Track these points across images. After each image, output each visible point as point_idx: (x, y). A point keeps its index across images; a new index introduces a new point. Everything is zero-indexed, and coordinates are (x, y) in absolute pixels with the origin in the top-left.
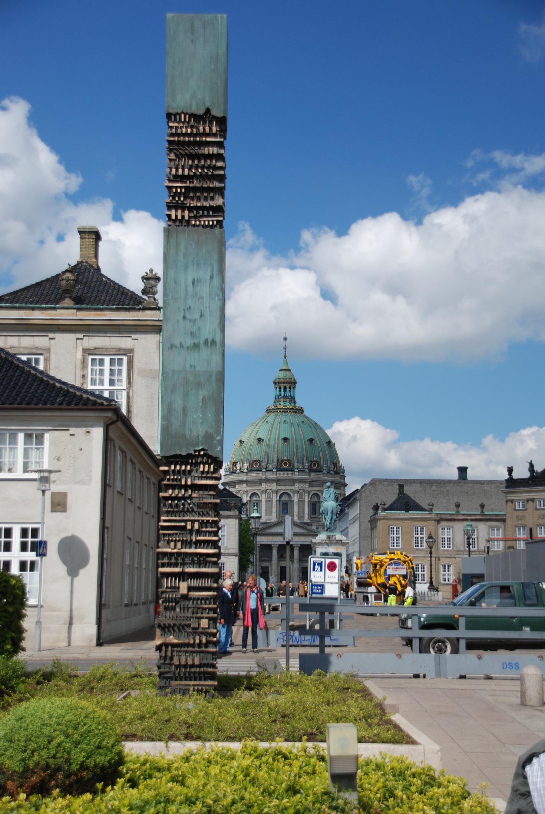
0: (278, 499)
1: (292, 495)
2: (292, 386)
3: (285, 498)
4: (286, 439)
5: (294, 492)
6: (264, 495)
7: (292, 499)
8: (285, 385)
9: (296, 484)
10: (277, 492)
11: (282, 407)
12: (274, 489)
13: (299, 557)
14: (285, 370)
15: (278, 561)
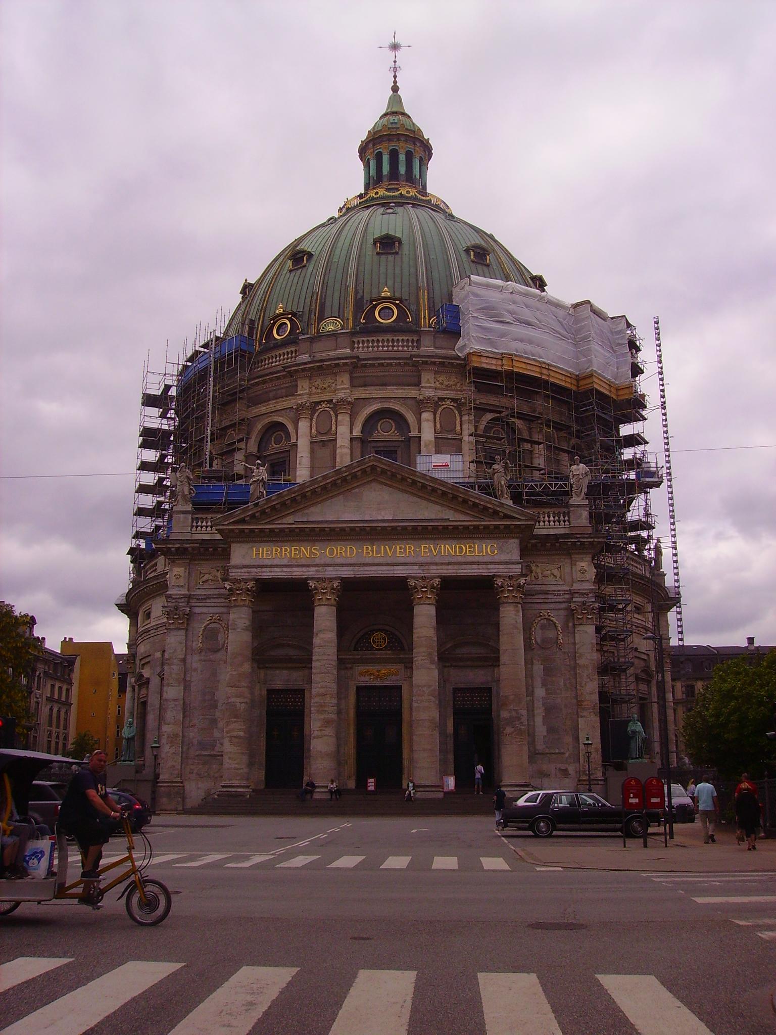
0: (357, 432)
1: (411, 418)
2: (418, 153)
3: (386, 433)
4: (388, 244)
5: (420, 406)
6: (303, 425)
7: (414, 433)
8: (393, 145)
9: (427, 379)
10: (353, 407)
11: (382, 192)
12: (341, 395)
13: (440, 644)
14: (394, 113)
15: (342, 664)
